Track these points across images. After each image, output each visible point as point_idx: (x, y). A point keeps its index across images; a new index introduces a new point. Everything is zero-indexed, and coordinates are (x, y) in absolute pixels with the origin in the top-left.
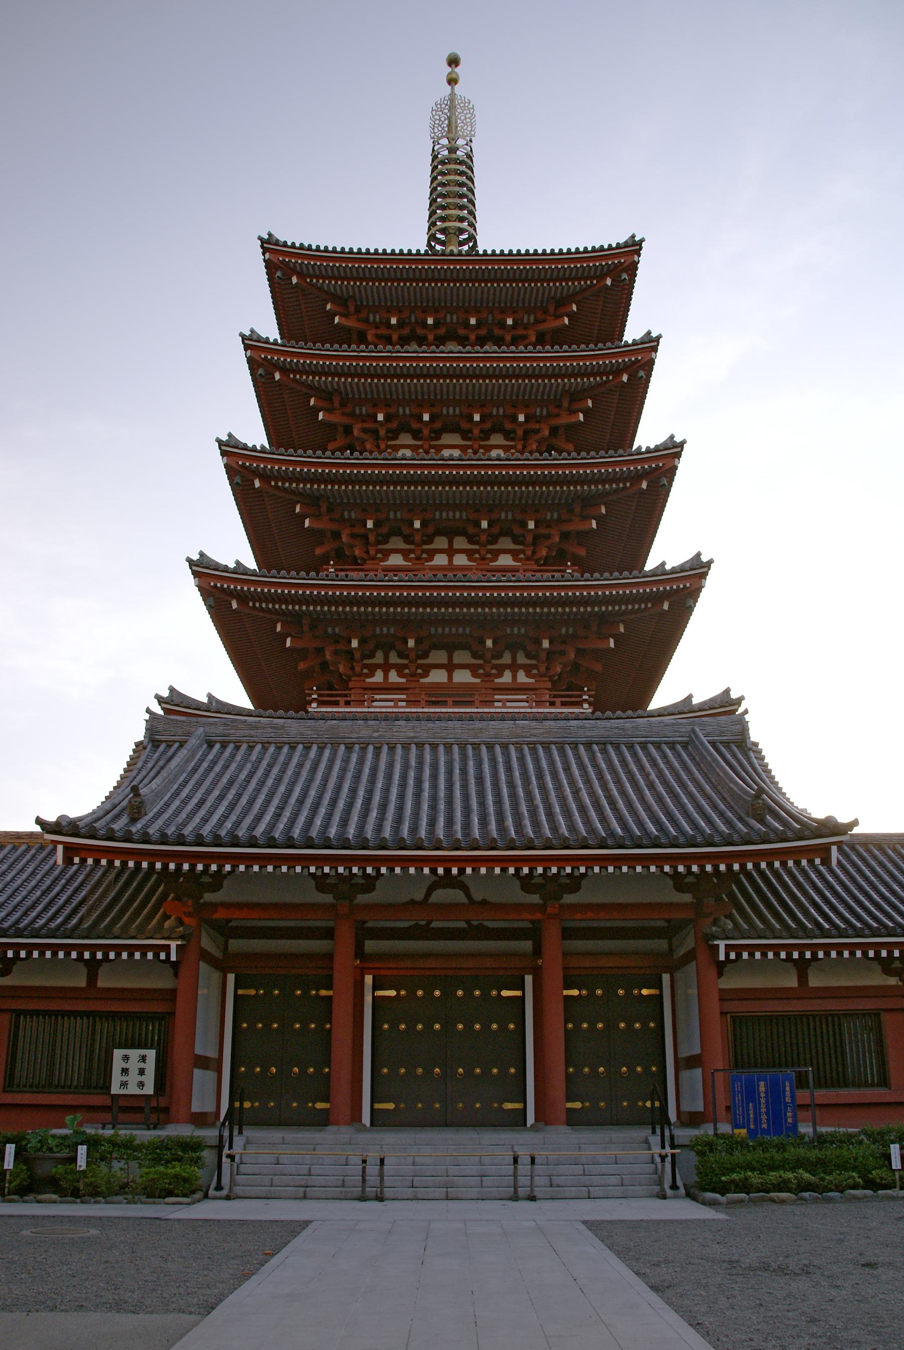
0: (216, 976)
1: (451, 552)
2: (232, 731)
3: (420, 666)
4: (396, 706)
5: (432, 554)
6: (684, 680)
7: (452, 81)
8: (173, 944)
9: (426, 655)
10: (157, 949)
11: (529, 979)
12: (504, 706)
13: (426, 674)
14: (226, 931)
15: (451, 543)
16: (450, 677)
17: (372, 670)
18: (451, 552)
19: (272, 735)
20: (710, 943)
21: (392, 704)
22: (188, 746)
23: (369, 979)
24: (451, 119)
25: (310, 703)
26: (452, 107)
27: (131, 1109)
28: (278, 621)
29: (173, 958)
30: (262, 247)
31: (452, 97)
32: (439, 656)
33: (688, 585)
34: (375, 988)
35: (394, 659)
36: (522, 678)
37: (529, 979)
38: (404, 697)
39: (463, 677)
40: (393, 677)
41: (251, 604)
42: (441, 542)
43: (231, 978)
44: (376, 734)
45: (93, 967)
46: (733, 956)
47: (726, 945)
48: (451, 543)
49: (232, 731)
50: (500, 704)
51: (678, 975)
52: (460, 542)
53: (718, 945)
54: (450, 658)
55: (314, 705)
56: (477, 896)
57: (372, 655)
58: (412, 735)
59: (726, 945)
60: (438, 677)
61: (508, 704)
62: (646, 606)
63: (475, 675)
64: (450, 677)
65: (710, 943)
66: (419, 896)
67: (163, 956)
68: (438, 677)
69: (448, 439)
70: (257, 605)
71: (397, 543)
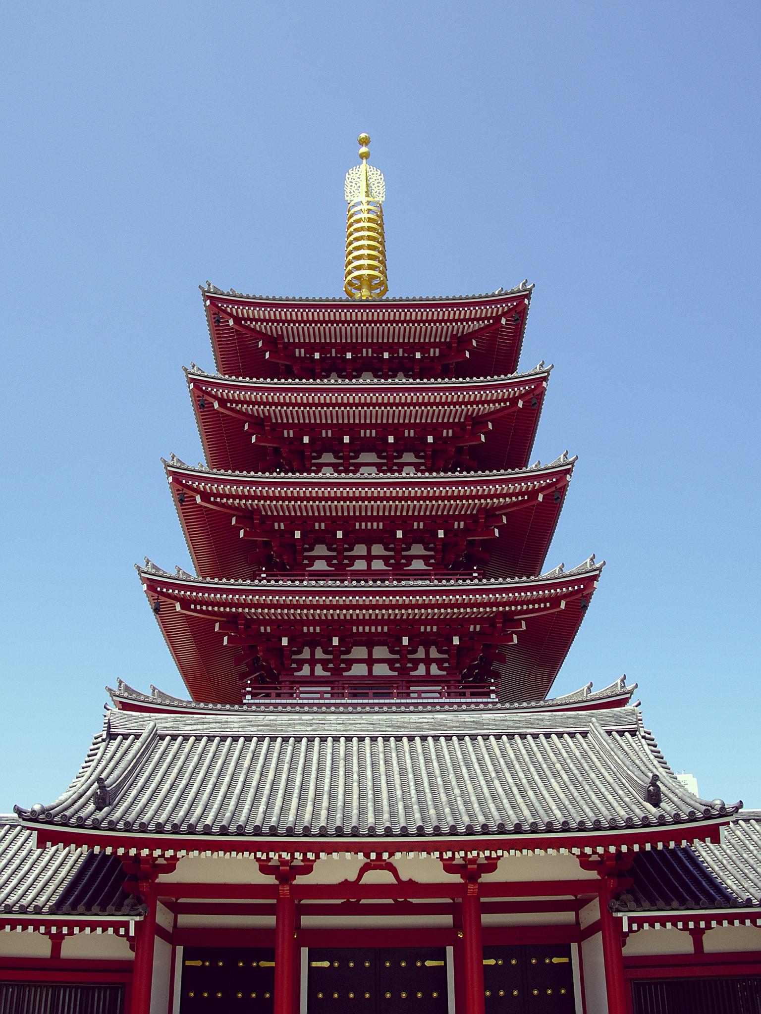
0: (168, 947)
2: (181, 726)
3: (344, 661)
4: (322, 698)
8: (132, 920)
9: (348, 652)
10: (116, 926)
11: (450, 950)
12: (419, 697)
13: (349, 669)
14: (177, 909)
15: (369, 550)
16: (370, 670)
17: (301, 663)
19: (217, 729)
20: (615, 915)
21: (318, 696)
22: (141, 739)
23: (305, 951)
25: (244, 695)
28: (217, 621)
29: (132, 933)
30: (204, 295)
32: (360, 652)
33: (582, 587)
34: (310, 961)
35: (319, 654)
36: (434, 670)
37: (450, 950)
38: (329, 689)
40: (319, 671)
41: (193, 607)
43: (180, 950)
44: (309, 729)
45: (56, 940)
46: (635, 927)
47: (629, 918)
48: (369, 550)
49: (181, 726)
50: (416, 695)
51: (584, 944)
53: (621, 918)
54: (370, 653)
55: (249, 697)
56: (404, 877)
57: (300, 652)
58: (342, 729)
59: (629, 918)
61: (423, 695)
62: (545, 606)
63: (392, 669)
64: (370, 670)
65: (615, 915)
66: (352, 877)
67: (122, 931)
68: (360, 670)
69: (365, 457)
70: (198, 607)
71: (321, 550)
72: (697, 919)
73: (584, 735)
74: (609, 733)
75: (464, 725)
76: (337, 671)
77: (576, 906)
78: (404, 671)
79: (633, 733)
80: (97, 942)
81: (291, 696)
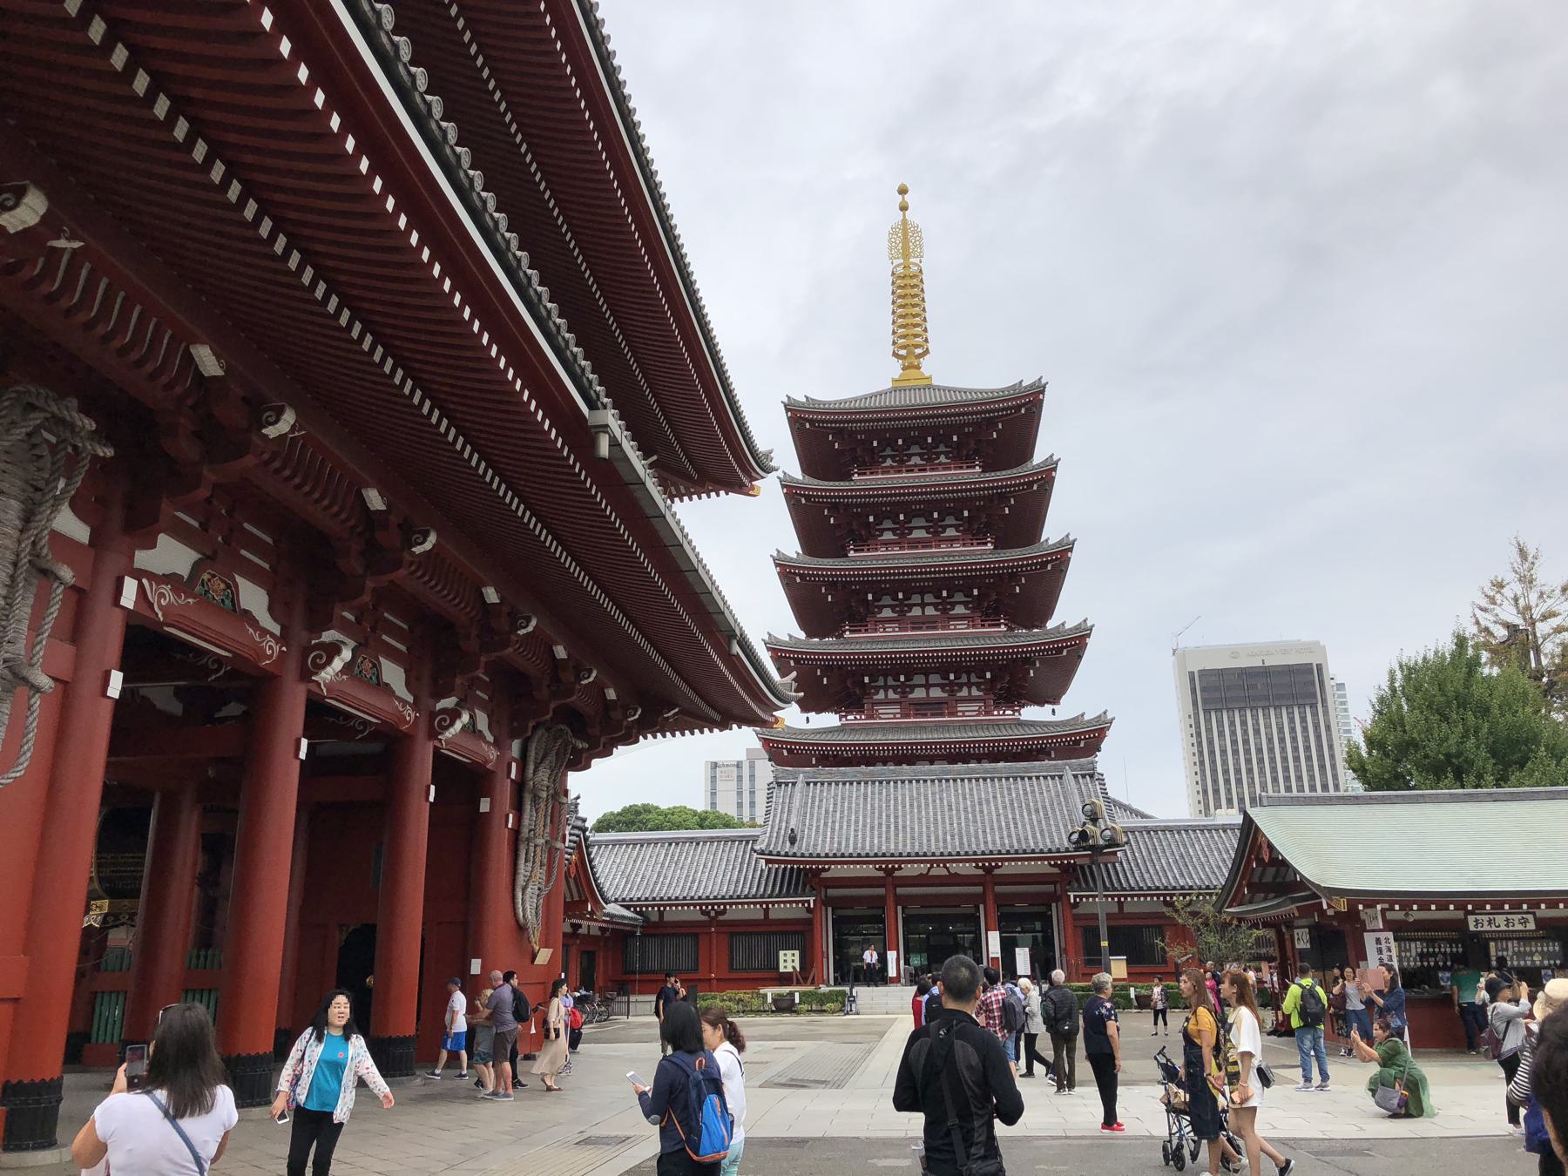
1: (923, 605)
5: (911, 607)
6: (1077, 702)
7: (904, 208)
10: (803, 902)
17: (877, 689)
18: (923, 605)
24: (906, 239)
26: (905, 231)
27: (786, 979)
31: (904, 221)
36: (975, 692)
39: (936, 693)
40: (891, 695)
42: (916, 599)
52: (929, 598)
60: (919, 693)
68: (919, 693)
72: (1119, 897)
73: (1060, 777)
74: (1075, 776)
75: (986, 771)
76: (904, 694)
77: (1055, 883)
78: (952, 693)
79: (1092, 776)
80: (788, 909)
81: (871, 717)
